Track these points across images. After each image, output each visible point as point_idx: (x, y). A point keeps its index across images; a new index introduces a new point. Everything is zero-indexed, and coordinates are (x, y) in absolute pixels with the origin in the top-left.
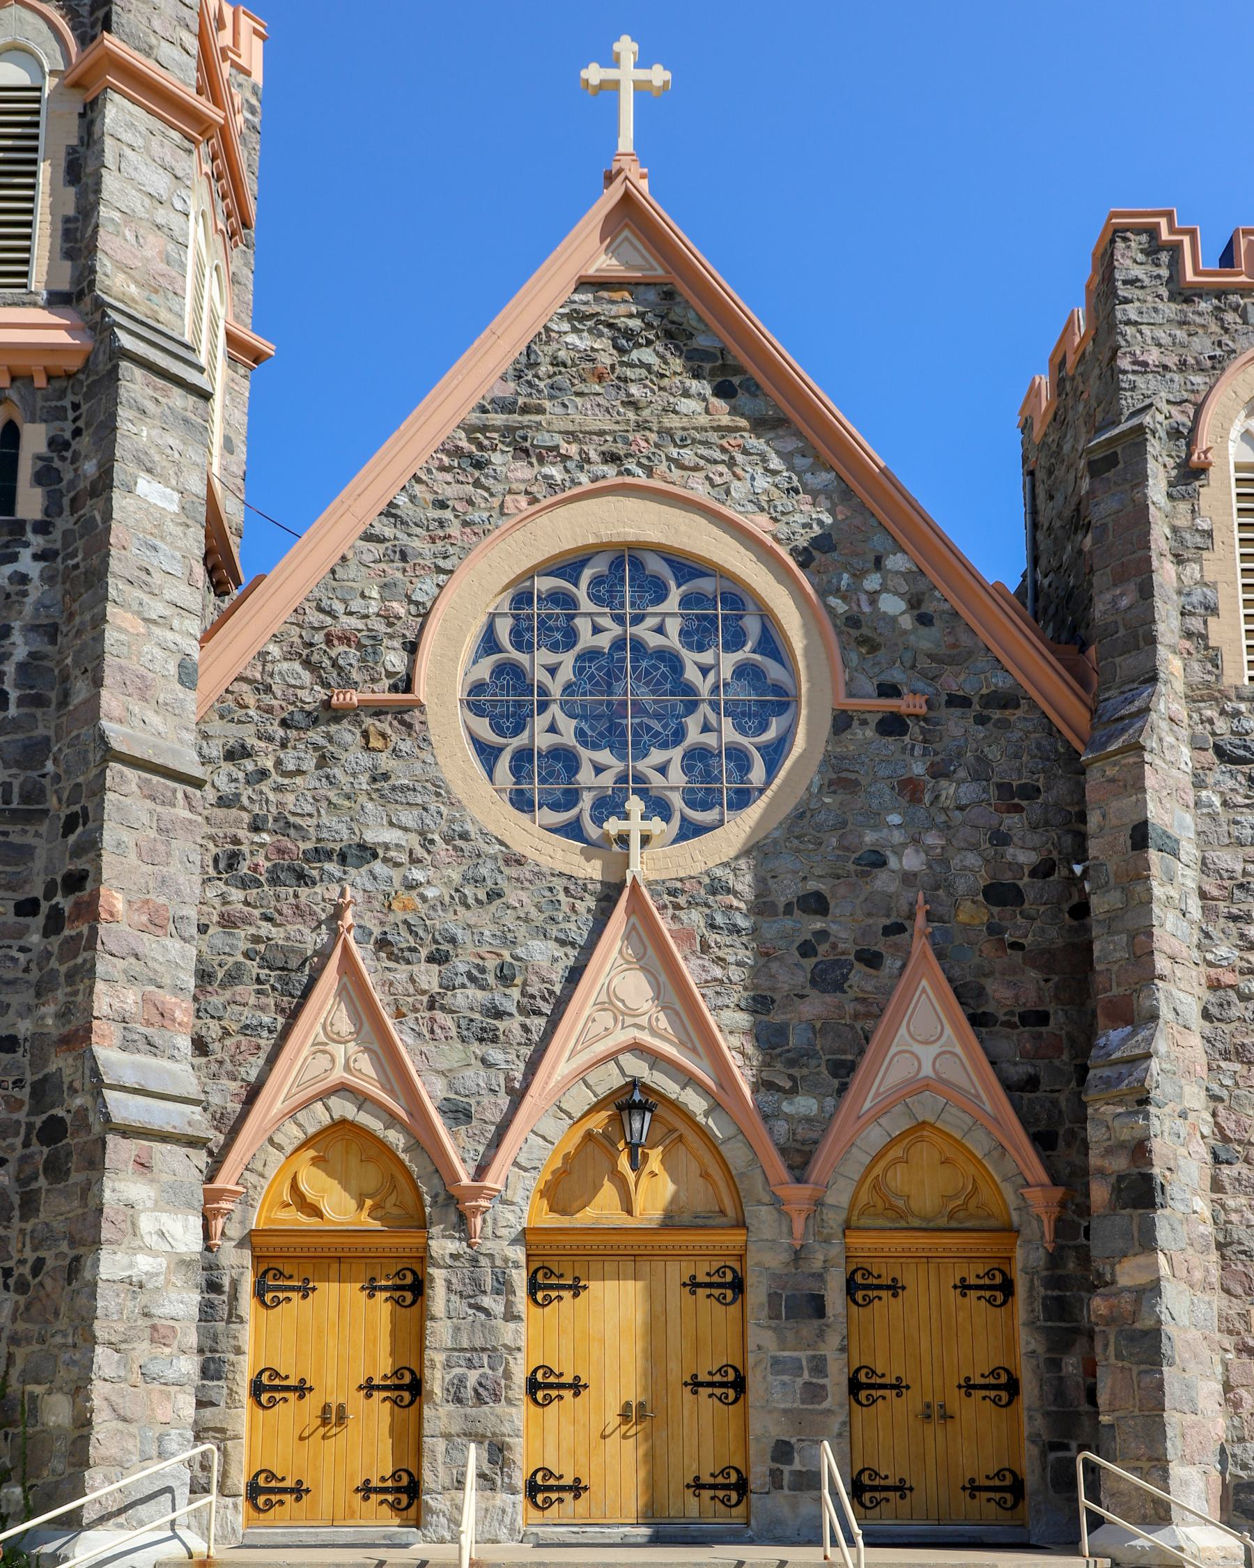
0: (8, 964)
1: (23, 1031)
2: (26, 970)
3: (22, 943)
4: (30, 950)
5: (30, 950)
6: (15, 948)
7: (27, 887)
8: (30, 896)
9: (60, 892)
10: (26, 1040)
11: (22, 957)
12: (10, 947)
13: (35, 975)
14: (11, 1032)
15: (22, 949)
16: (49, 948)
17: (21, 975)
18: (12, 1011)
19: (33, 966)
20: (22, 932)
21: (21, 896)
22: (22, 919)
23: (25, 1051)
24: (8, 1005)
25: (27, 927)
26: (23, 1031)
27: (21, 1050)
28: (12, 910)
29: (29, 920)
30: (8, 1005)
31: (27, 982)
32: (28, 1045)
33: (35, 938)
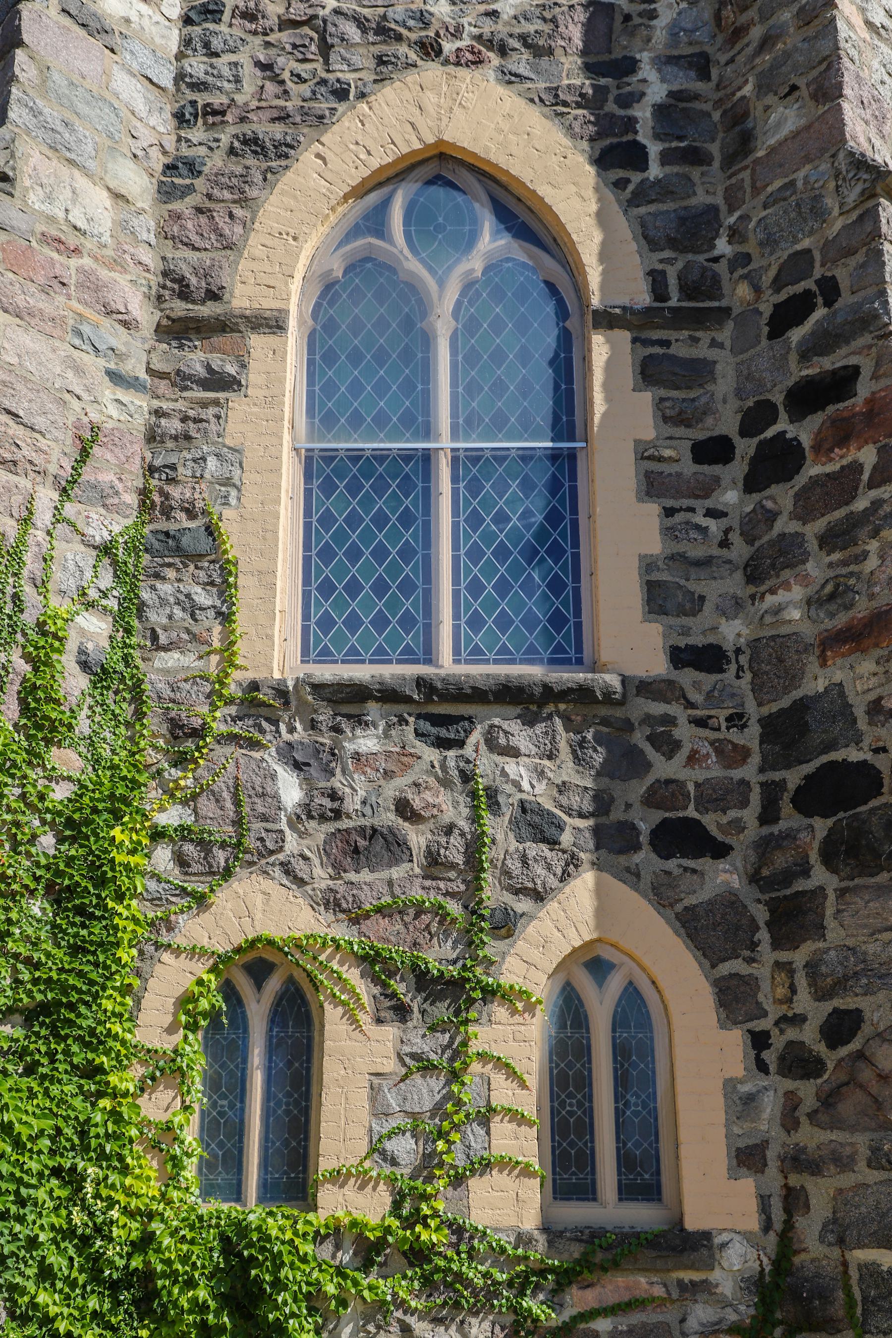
0: (693, 534)
1: (731, 637)
2: (724, 543)
3: (709, 503)
4: (725, 515)
5: (725, 515)
6: (701, 511)
7: (709, 421)
8: (716, 433)
9: (783, 415)
10: (738, 651)
11: (712, 525)
12: (692, 510)
13: (740, 551)
14: (711, 639)
15: (711, 513)
16: (769, 504)
17: (716, 551)
18: (708, 607)
19: (735, 538)
20: (707, 489)
21: (700, 435)
22: (705, 468)
23: (740, 668)
24: (702, 598)
25: (717, 480)
26: (731, 637)
27: (733, 667)
28: (689, 455)
29: (717, 469)
30: (702, 598)
31: (729, 562)
32: (744, 660)
33: (730, 497)
